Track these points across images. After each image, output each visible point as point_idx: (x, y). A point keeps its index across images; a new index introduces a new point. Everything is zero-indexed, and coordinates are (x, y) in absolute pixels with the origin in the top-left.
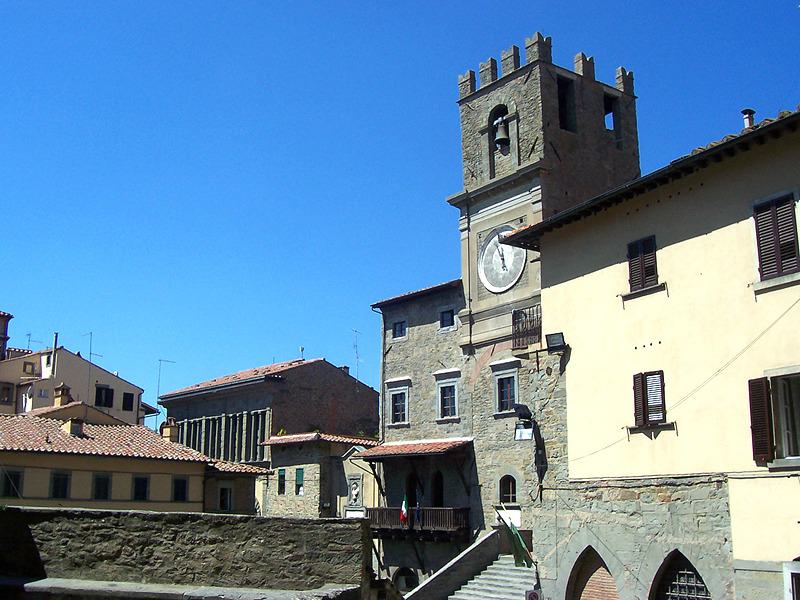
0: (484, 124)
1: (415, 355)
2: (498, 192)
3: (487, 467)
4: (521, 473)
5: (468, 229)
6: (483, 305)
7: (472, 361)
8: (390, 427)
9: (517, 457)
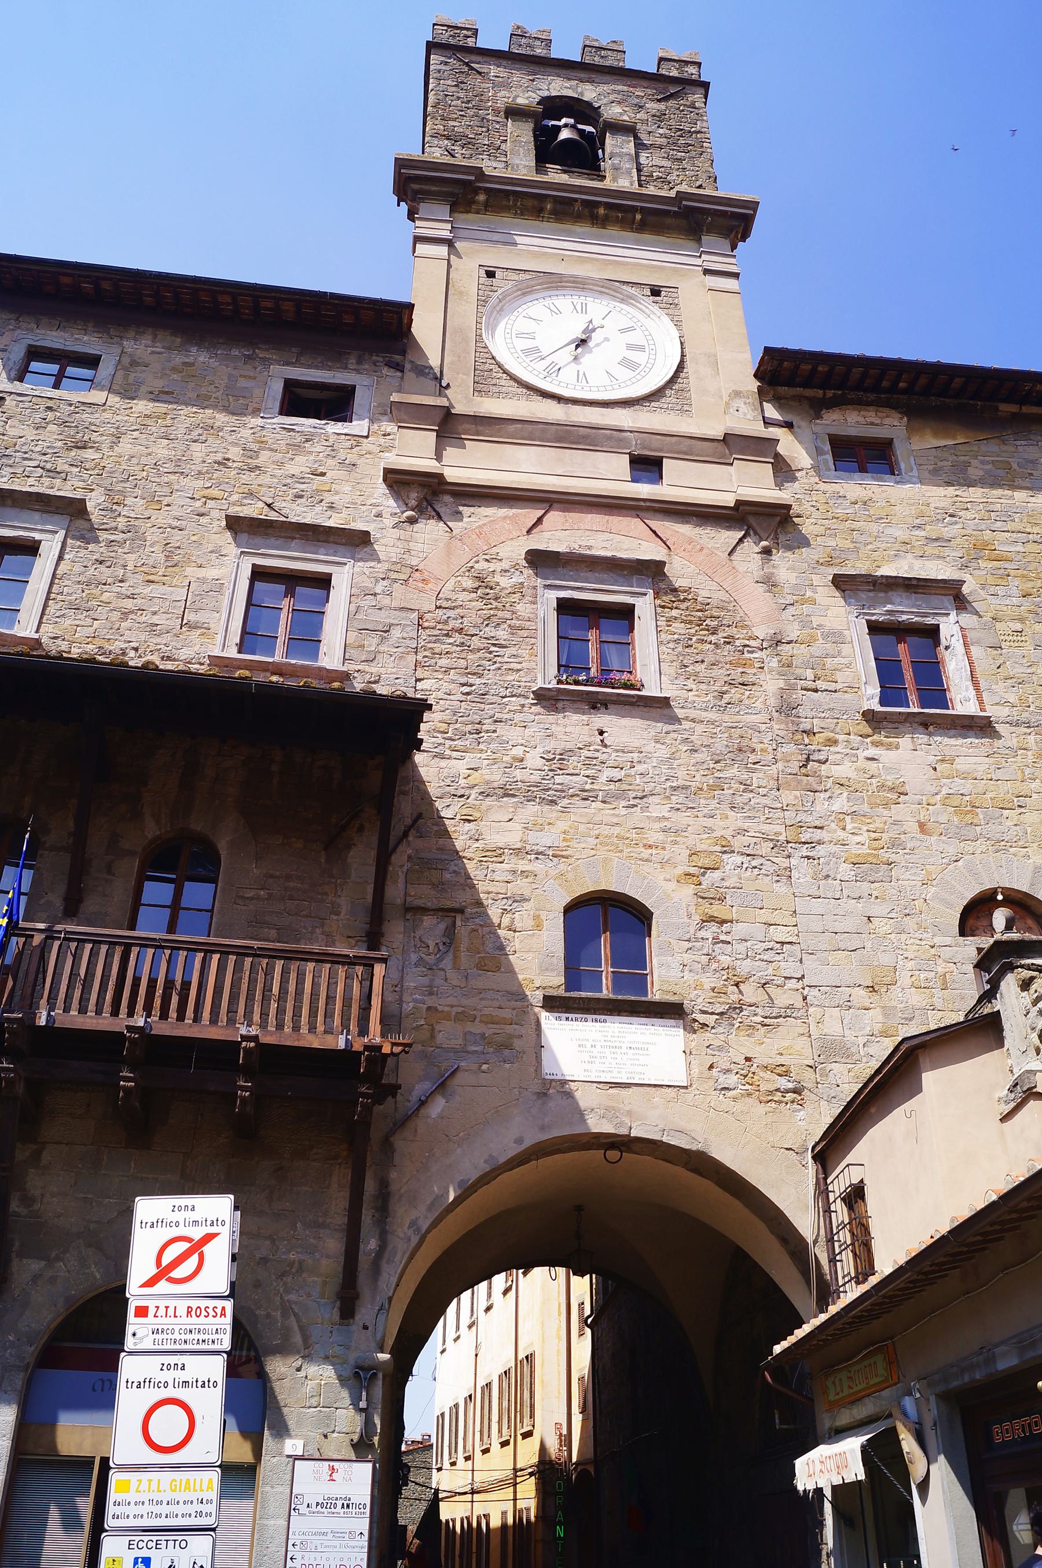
2: (577, 218)
3: (497, 853)
7: (430, 530)
9: (654, 837)
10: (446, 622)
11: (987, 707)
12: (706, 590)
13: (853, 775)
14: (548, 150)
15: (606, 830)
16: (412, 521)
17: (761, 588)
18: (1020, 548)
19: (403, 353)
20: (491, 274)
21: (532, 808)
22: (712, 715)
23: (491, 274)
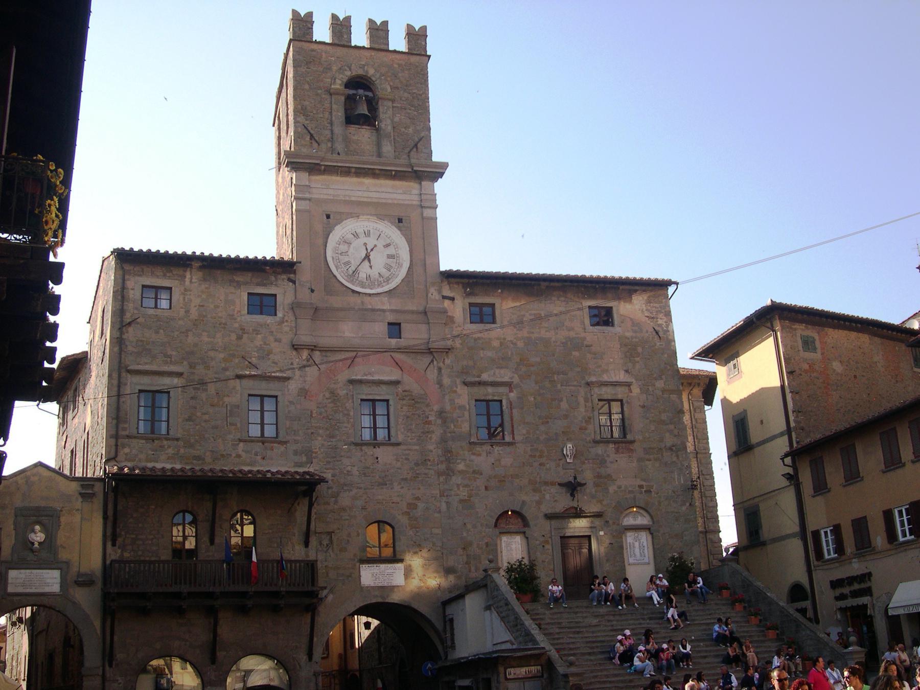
0: (338, 85)
1: (191, 339)
3: (344, 509)
4: (404, 520)
5: (310, 200)
6: (336, 301)
7: (312, 372)
8: (128, 437)
9: (395, 499)
10: (321, 414)
11: (516, 438)
12: (416, 388)
13: (464, 468)
14: (351, 119)
15: (380, 497)
16: (304, 366)
17: (437, 386)
18: (538, 359)
19: (295, 273)
20: (328, 217)
21: (355, 491)
22: (417, 447)
23: (328, 217)
